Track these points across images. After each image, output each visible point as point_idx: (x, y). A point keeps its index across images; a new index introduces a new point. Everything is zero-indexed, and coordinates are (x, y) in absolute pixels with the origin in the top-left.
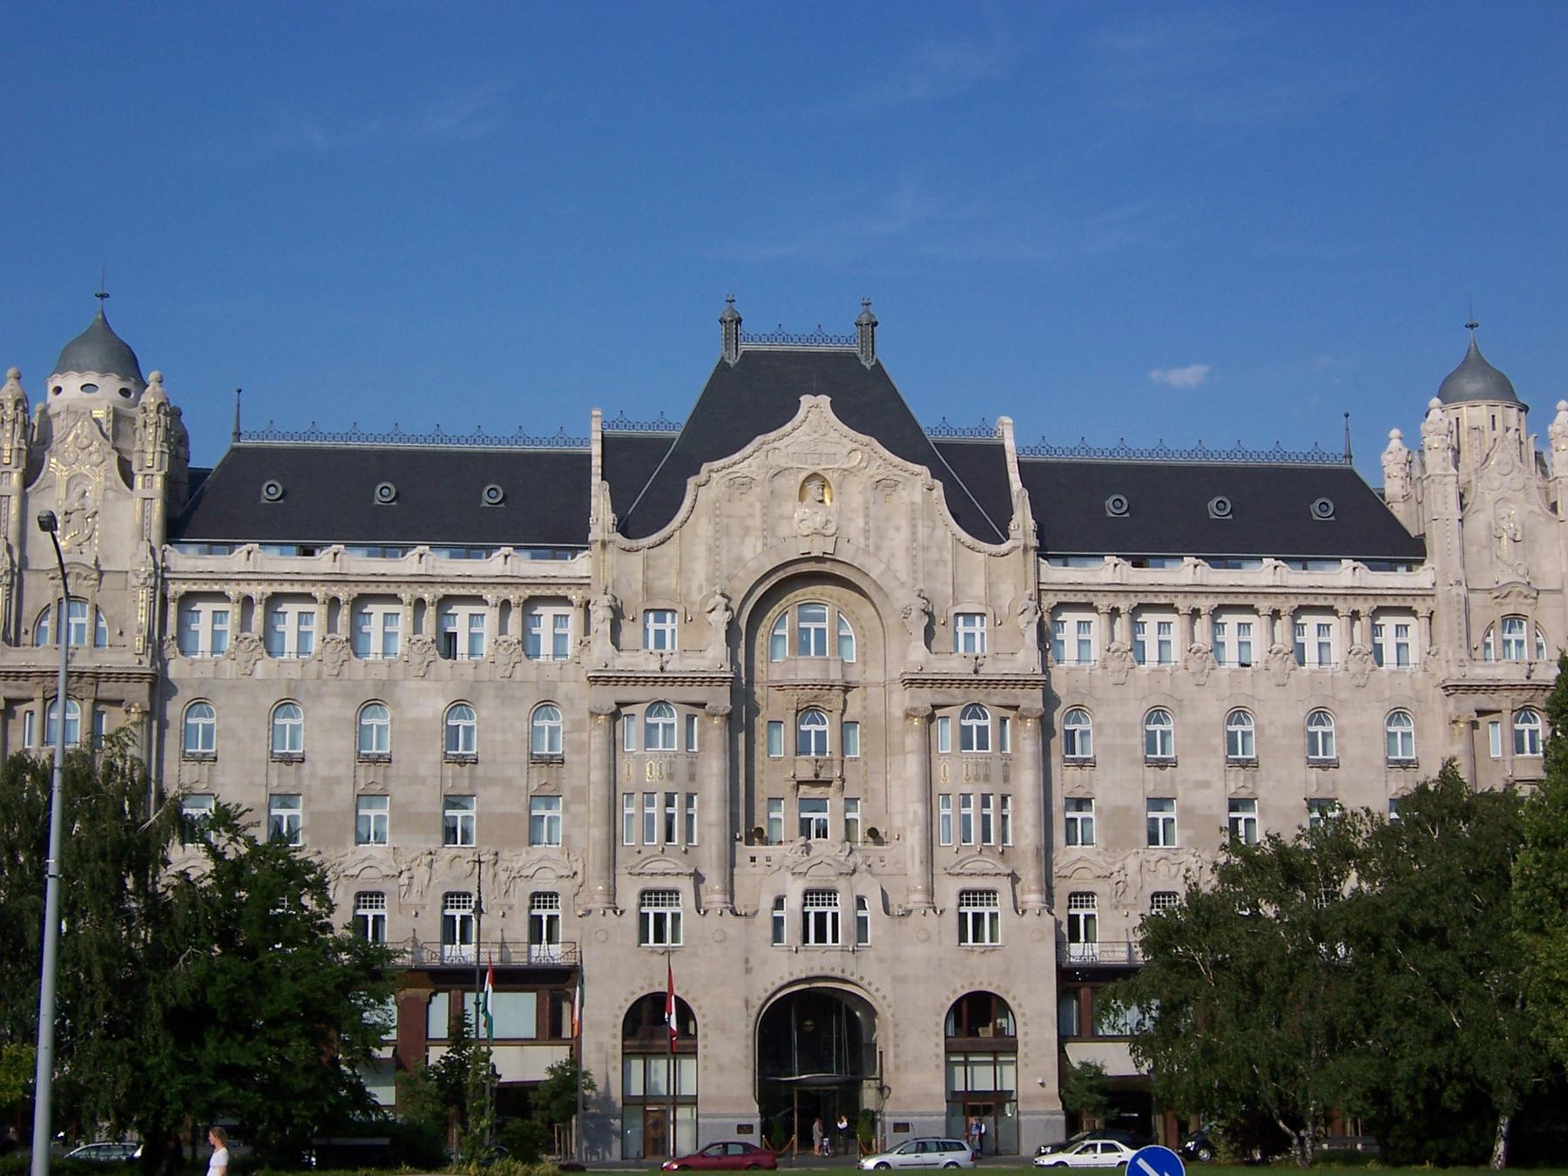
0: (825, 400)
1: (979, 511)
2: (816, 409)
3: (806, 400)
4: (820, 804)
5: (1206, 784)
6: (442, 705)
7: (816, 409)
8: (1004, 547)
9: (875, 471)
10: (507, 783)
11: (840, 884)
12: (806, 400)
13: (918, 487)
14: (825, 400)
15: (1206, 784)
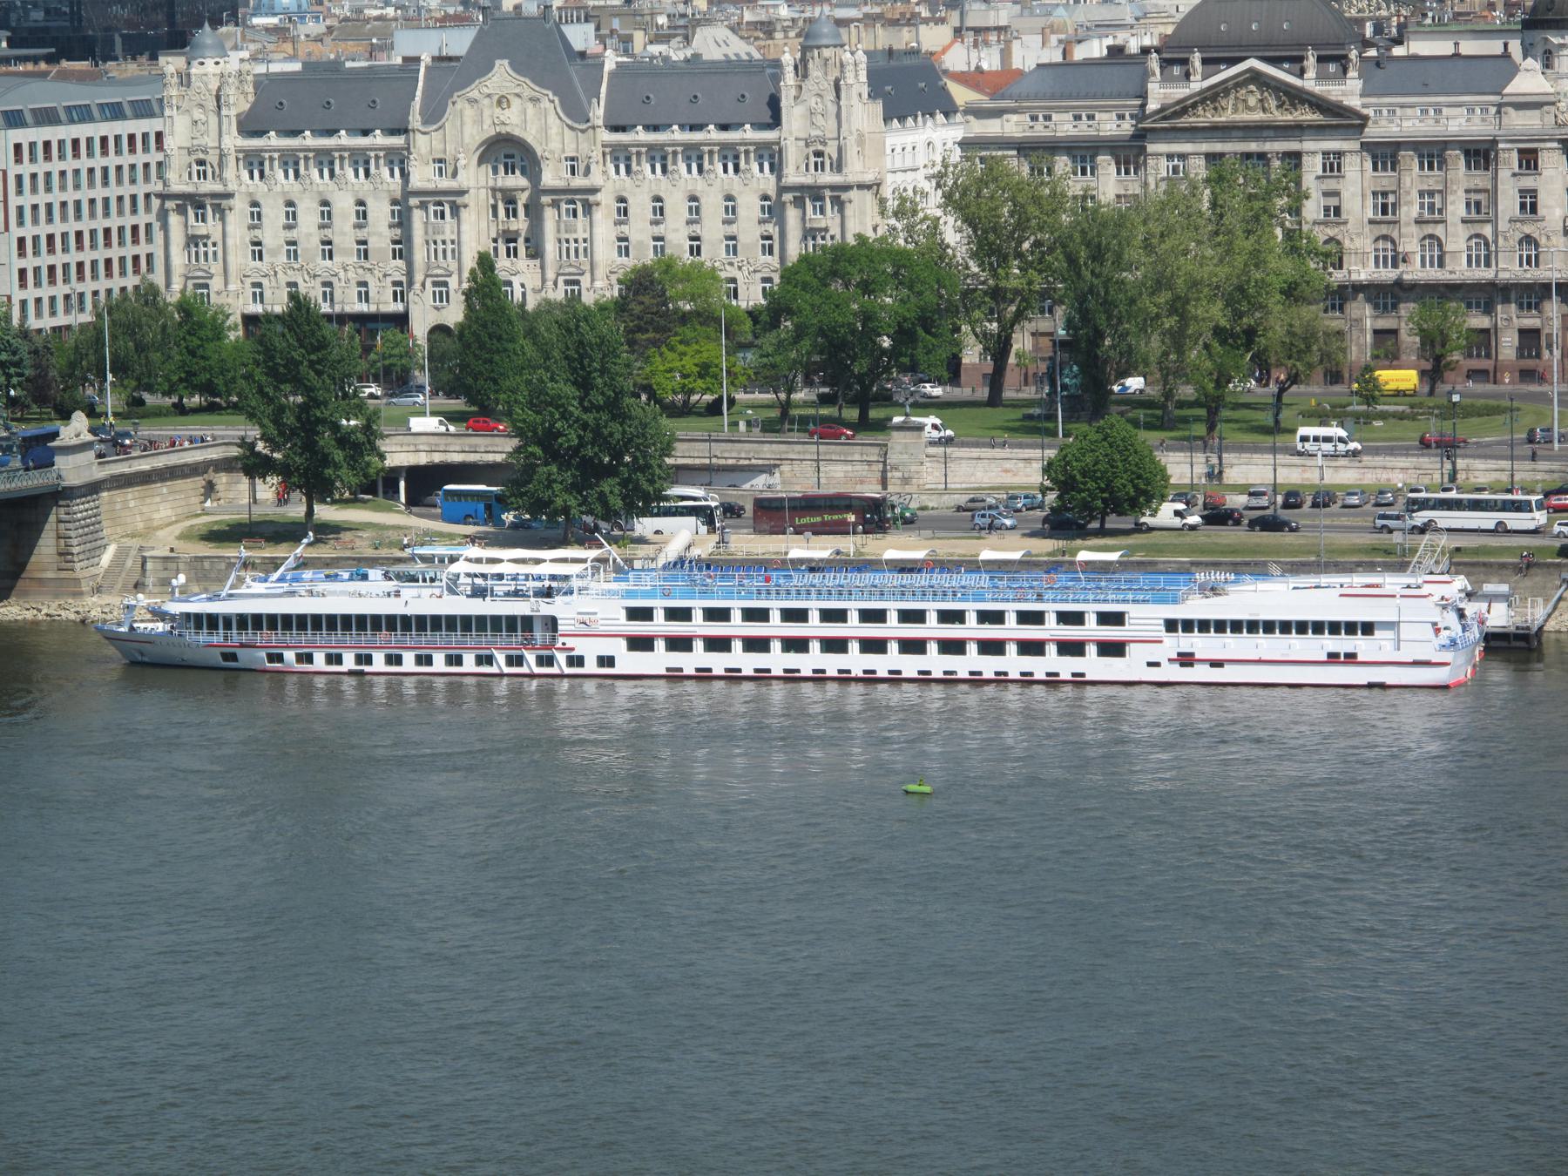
0: (506, 62)
1: (575, 112)
2: (502, 67)
3: (498, 62)
4: (515, 241)
5: (676, 230)
6: (352, 201)
7: (502, 67)
8: (584, 126)
9: (527, 93)
10: (380, 235)
11: (513, 279)
12: (498, 62)
13: (550, 103)
14: (506, 62)
15: (676, 230)
